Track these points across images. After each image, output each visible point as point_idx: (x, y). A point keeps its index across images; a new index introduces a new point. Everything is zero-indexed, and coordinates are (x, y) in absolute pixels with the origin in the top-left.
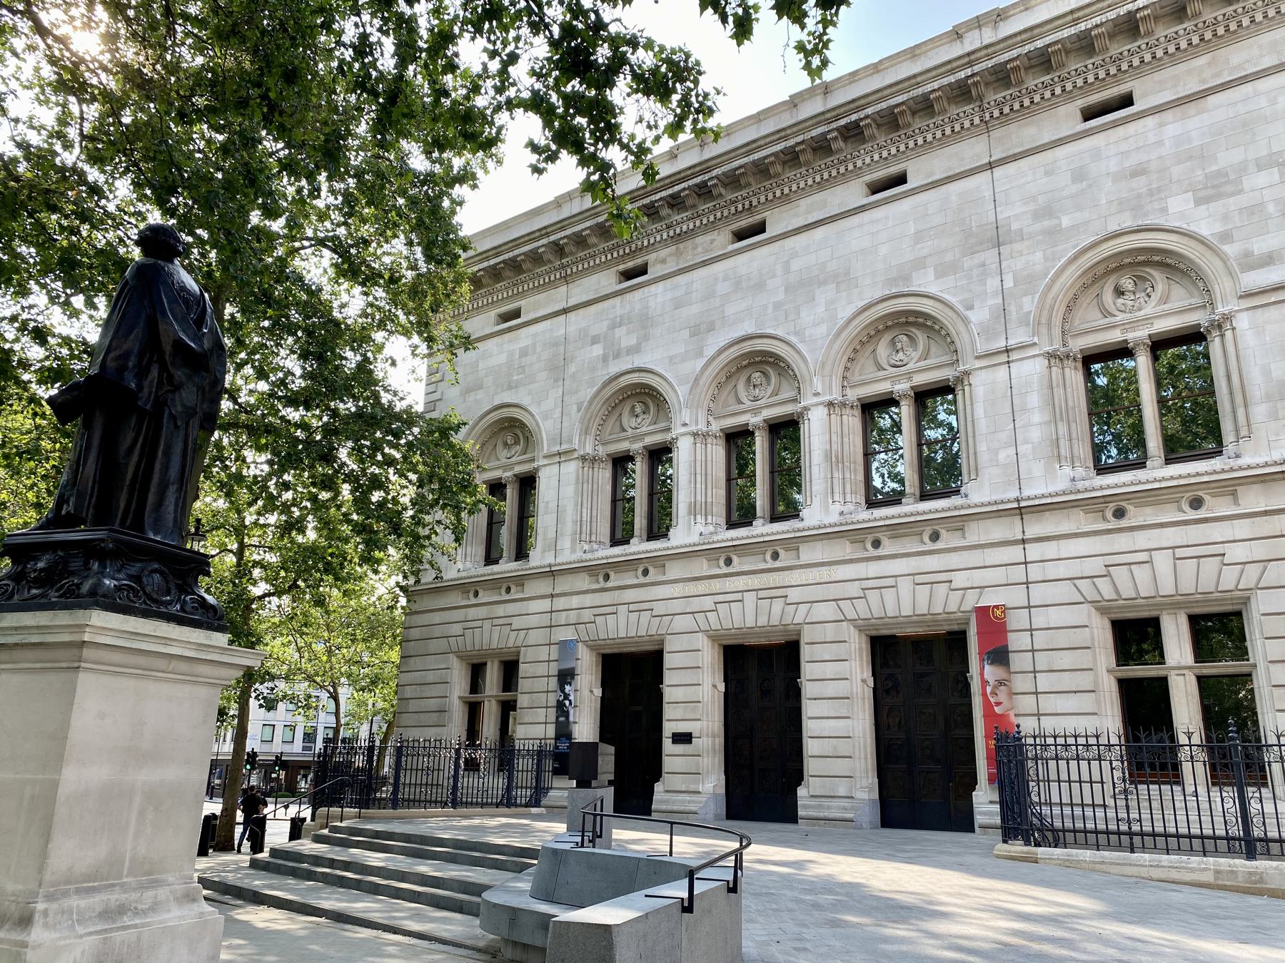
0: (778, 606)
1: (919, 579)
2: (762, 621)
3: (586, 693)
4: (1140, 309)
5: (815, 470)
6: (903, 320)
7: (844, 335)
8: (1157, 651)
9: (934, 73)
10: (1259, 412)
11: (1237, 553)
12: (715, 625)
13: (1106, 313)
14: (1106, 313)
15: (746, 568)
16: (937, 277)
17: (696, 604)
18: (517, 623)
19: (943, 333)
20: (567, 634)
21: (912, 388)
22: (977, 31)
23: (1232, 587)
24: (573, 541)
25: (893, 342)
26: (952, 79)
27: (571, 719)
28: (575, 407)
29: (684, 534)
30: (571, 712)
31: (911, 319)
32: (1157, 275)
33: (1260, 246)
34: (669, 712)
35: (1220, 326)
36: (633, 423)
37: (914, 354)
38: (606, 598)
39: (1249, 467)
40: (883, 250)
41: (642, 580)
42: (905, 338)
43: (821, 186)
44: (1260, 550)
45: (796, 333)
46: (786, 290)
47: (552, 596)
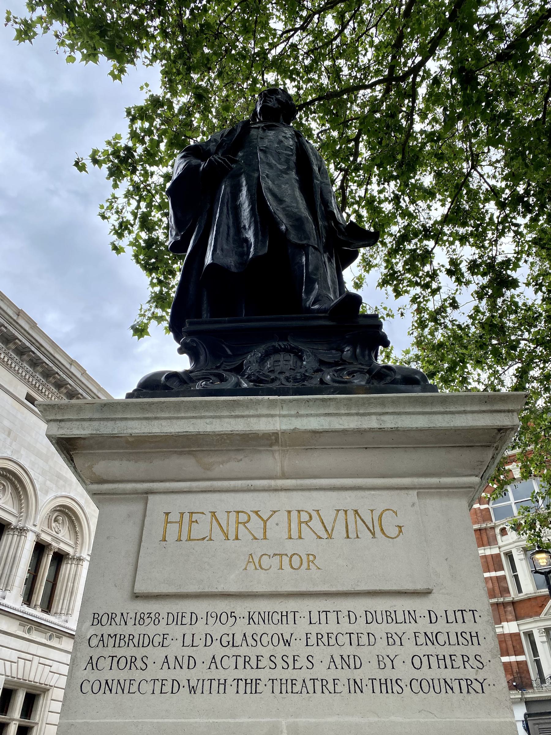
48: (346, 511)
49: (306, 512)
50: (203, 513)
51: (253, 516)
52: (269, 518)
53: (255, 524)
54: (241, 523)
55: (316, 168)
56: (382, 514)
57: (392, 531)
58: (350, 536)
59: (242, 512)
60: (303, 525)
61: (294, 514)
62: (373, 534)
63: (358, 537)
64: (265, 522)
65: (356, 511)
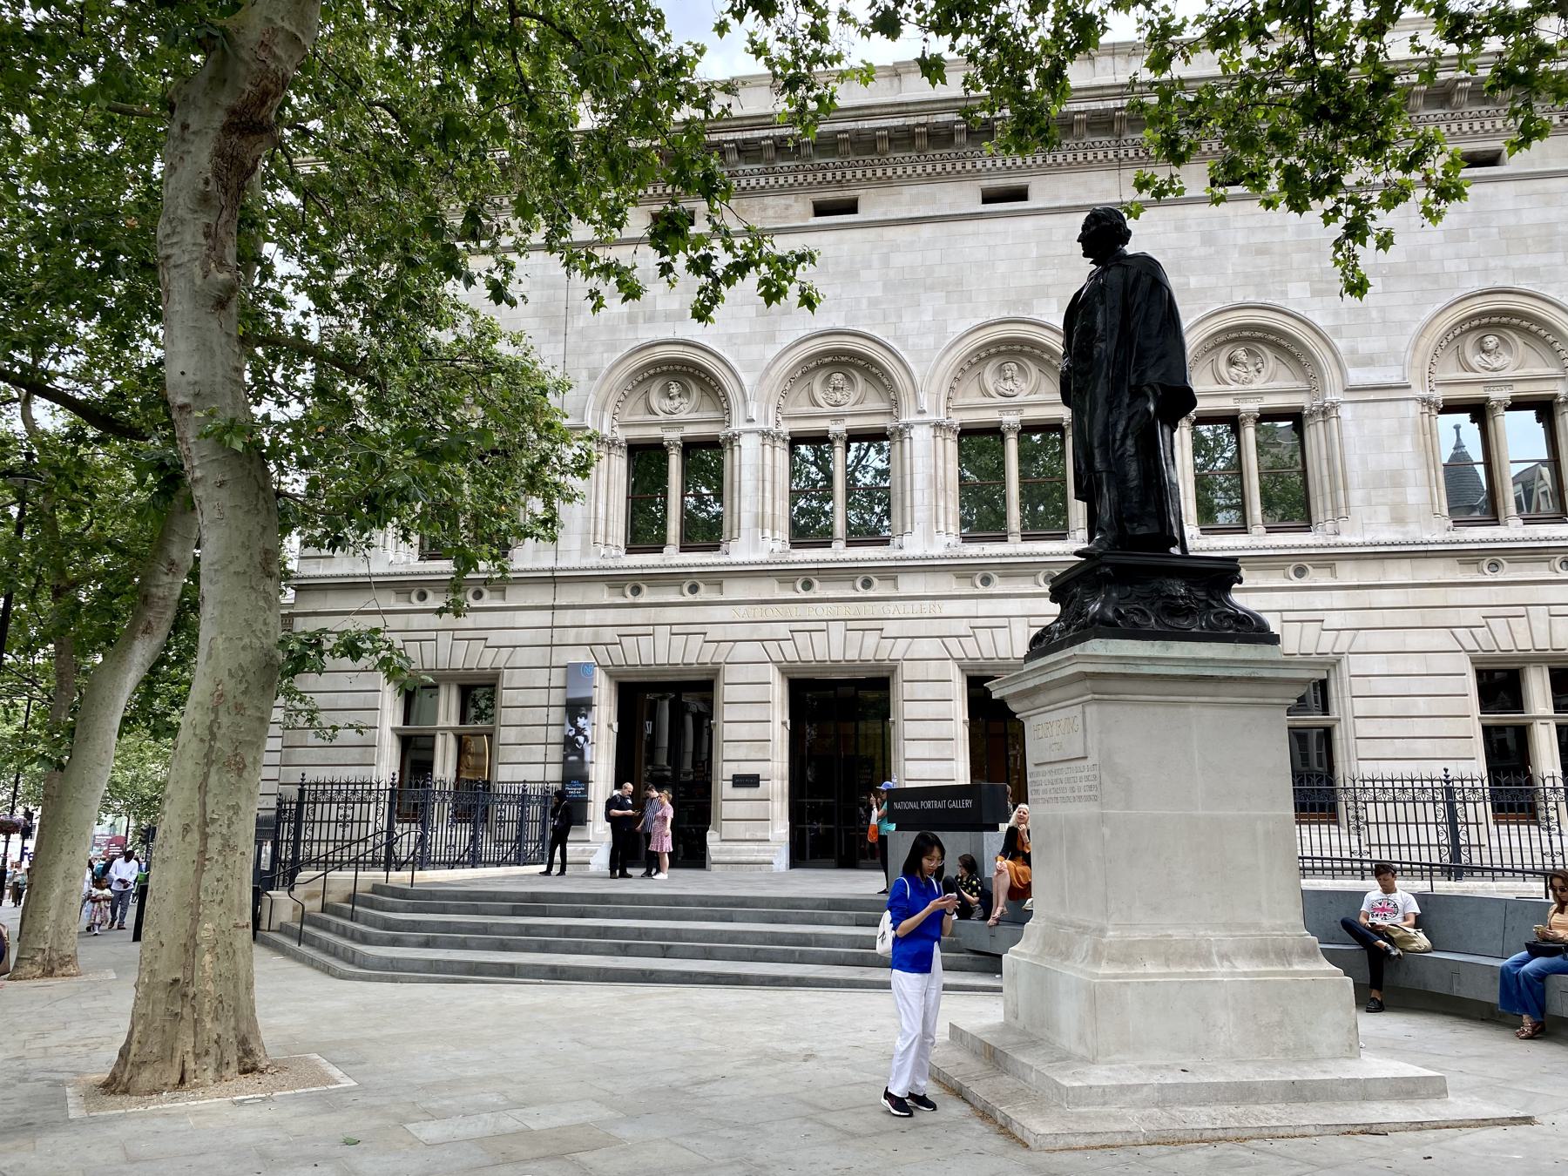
0: (871, 639)
2: (852, 655)
3: (604, 726)
5: (918, 495)
6: (1017, 347)
7: (953, 352)
8: (1517, 703)
9: (1083, 94)
10: (1356, 496)
11: (1334, 620)
12: (791, 655)
14: (1220, 380)
15: (831, 594)
17: (765, 631)
18: (495, 638)
20: (580, 656)
22: (1109, 59)
24: (585, 542)
25: (1000, 369)
26: (1100, 105)
27: (587, 758)
28: (584, 375)
29: (742, 550)
30: (588, 749)
31: (1027, 349)
32: (1269, 354)
33: (1365, 346)
34: (729, 751)
35: (1324, 413)
36: (667, 404)
38: (638, 616)
39: (1344, 546)
40: (1002, 268)
41: (690, 598)
43: (930, 178)
44: (1352, 619)
45: (896, 338)
46: (885, 285)
47: (553, 607)
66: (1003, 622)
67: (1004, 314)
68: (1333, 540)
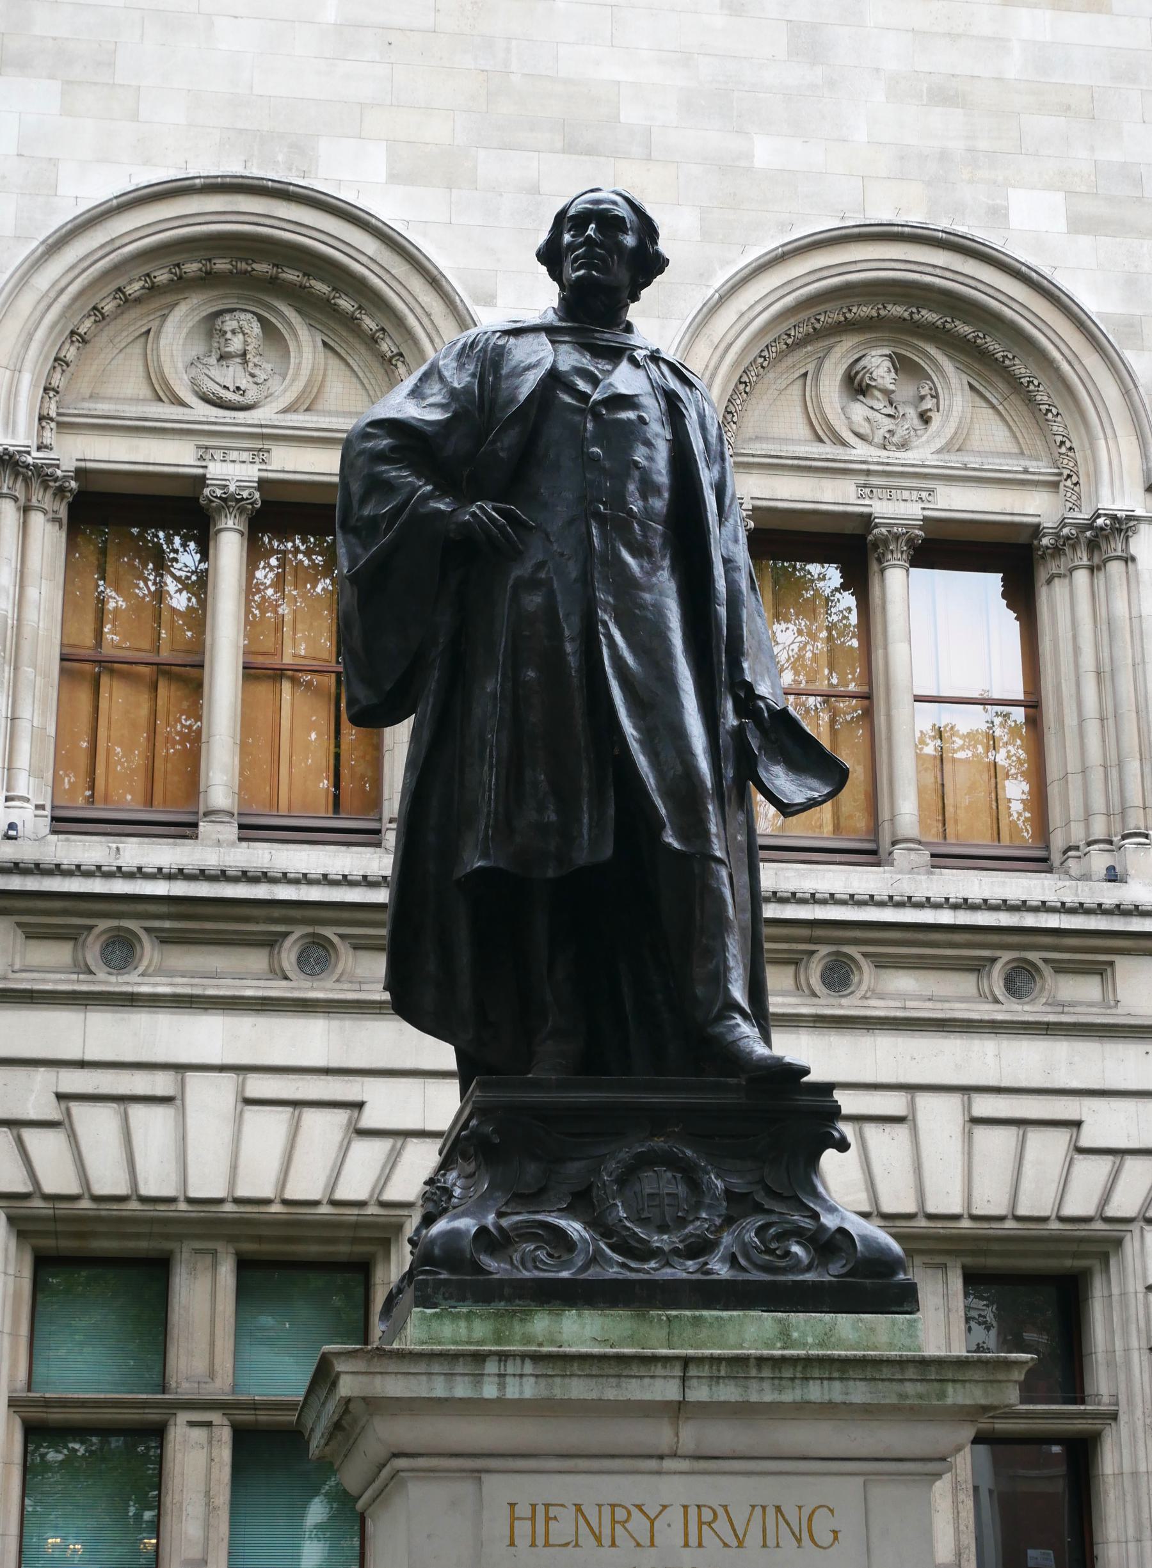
1: (258, 1086)
4: (904, 445)
13: (824, 431)
16: (394, 178)
19: (385, 346)
21: (263, 484)
23: (1089, 1210)
25: (211, 326)
31: (291, 275)
35: (1093, 546)
37: (275, 385)
42: (256, 328)
48: (764, 1508)
49: (710, 1507)
50: (562, 1505)
51: (635, 1512)
52: (657, 1517)
53: (638, 1523)
54: (618, 1522)
55: (721, 585)
56: (813, 1512)
57: (825, 1538)
58: (768, 1543)
59: (619, 1505)
60: (705, 1527)
61: (693, 1511)
62: (799, 1540)
63: (778, 1546)
64: (652, 1522)
65: (778, 1509)
66: (161, 1084)
67: (232, 167)
68: (1110, 895)
